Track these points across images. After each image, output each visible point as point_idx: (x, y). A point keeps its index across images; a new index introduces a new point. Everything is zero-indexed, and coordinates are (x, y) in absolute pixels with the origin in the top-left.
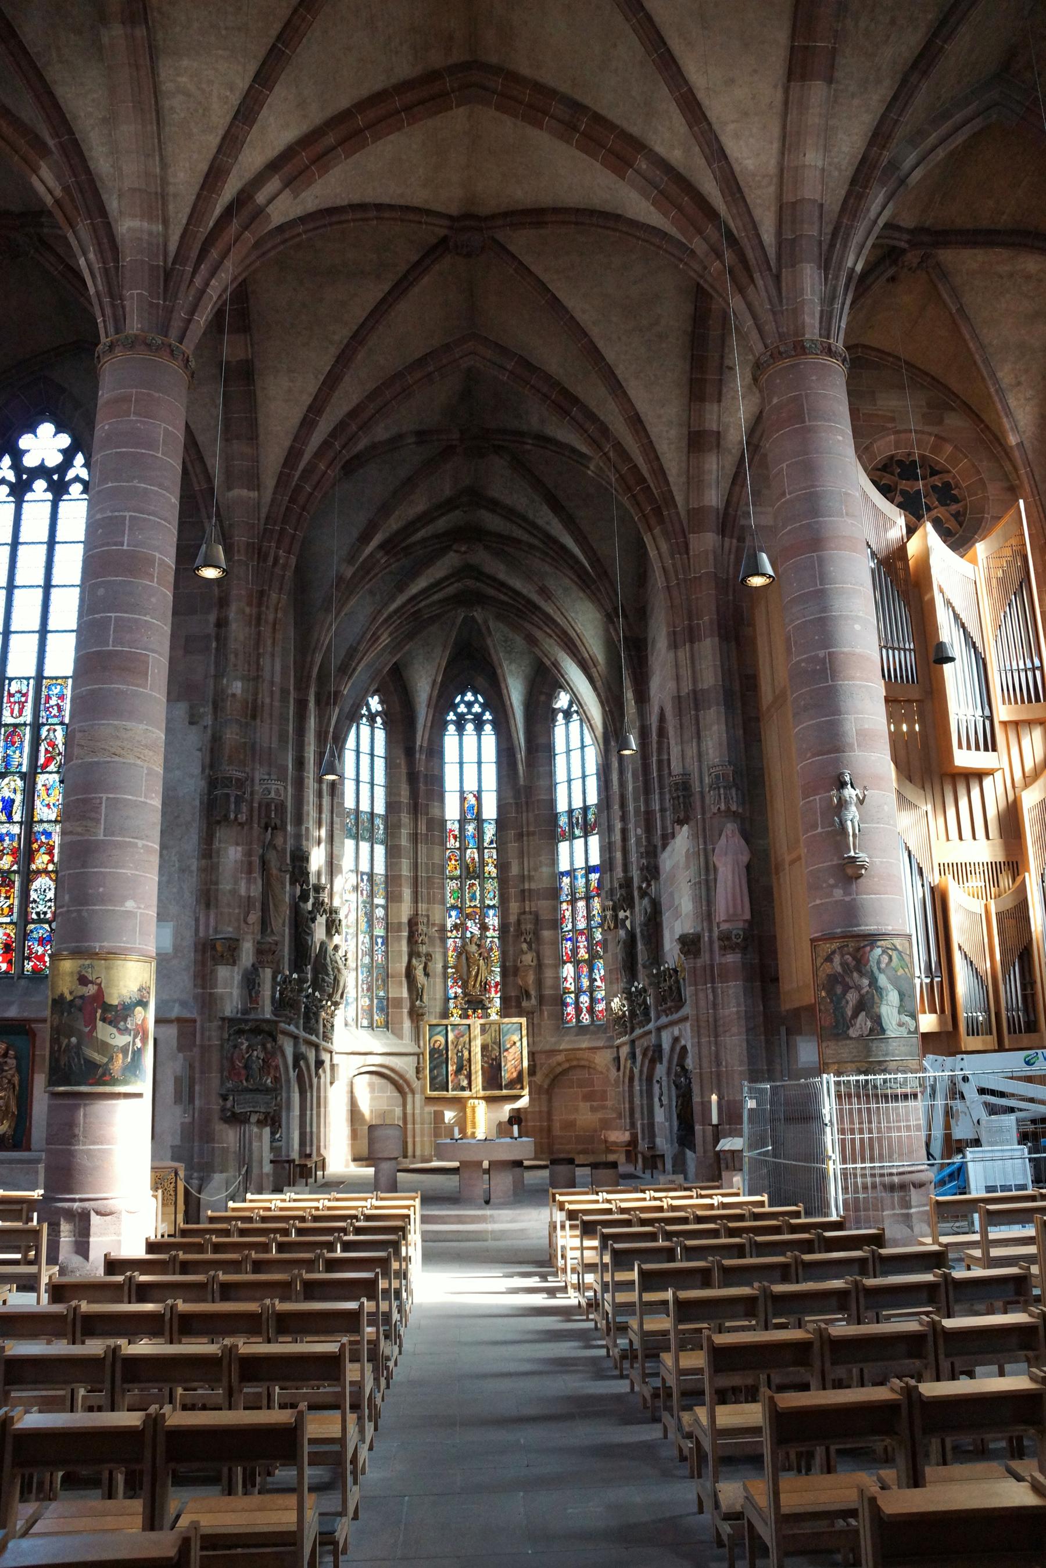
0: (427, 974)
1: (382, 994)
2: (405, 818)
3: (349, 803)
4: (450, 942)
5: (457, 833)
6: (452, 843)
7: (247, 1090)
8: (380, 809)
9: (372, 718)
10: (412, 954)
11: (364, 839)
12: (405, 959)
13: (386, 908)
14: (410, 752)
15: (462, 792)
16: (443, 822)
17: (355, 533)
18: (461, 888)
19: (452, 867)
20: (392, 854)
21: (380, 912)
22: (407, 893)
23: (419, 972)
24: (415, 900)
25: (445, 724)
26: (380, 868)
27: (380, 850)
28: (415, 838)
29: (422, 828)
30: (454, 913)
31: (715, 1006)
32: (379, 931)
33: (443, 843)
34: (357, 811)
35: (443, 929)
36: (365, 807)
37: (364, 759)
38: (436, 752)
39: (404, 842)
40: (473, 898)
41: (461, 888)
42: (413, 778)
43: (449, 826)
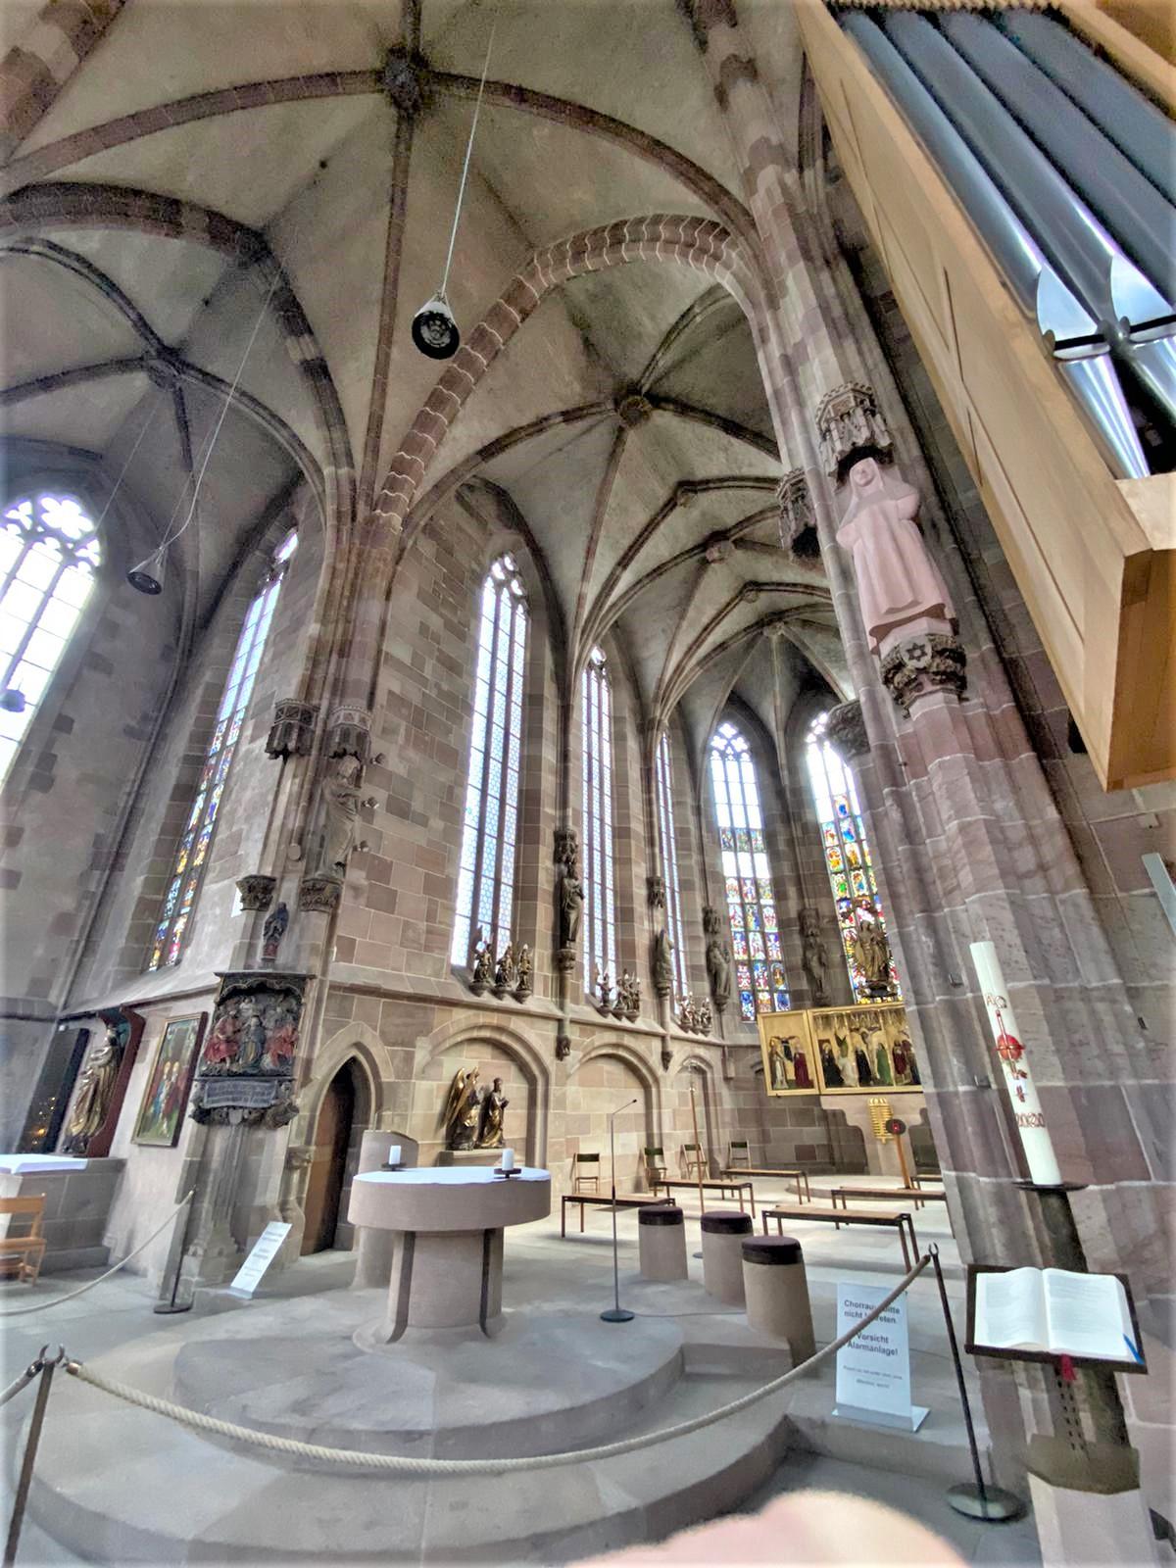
0: (822, 964)
1: (782, 987)
2: (779, 827)
3: (723, 821)
4: (846, 932)
5: (833, 832)
6: (829, 842)
7: (232, 1075)
8: (756, 823)
9: (737, 756)
10: (807, 947)
11: (742, 850)
12: (800, 951)
13: (774, 907)
14: (775, 773)
15: (831, 797)
16: (817, 828)
17: (583, 554)
18: (847, 880)
19: (834, 864)
20: (774, 857)
21: (769, 912)
22: (792, 891)
23: (814, 964)
24: (801, 896)
25: (803, 746)
26: (764, 874)
27: (762, 859)
28: (791, 842)
29: (797, 833)
30: (844, 904)
31: (910, 835)
32: (771, 928)
33: (820, 843)
34: (733, 831)
35: (834, 920)
36: (740, 823)
37: (735, 787)
38: (795, 769)
39: (782, 846)
40: (861, 887)
41: (847, 880)
42: (780, 793)
43: (825, 828)
